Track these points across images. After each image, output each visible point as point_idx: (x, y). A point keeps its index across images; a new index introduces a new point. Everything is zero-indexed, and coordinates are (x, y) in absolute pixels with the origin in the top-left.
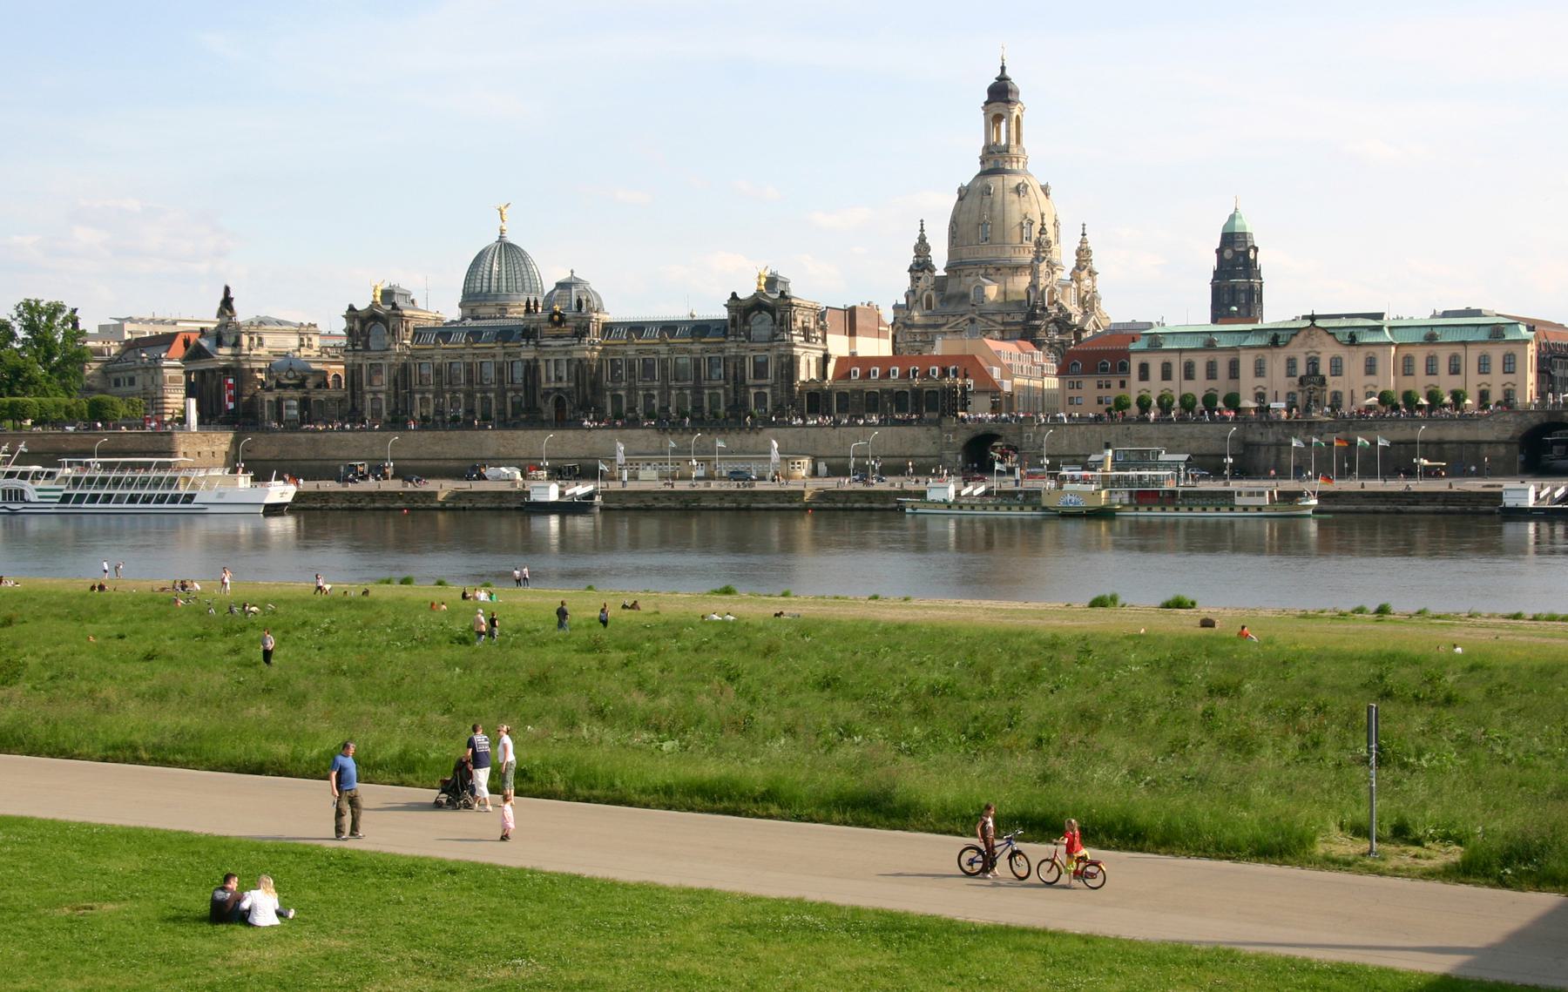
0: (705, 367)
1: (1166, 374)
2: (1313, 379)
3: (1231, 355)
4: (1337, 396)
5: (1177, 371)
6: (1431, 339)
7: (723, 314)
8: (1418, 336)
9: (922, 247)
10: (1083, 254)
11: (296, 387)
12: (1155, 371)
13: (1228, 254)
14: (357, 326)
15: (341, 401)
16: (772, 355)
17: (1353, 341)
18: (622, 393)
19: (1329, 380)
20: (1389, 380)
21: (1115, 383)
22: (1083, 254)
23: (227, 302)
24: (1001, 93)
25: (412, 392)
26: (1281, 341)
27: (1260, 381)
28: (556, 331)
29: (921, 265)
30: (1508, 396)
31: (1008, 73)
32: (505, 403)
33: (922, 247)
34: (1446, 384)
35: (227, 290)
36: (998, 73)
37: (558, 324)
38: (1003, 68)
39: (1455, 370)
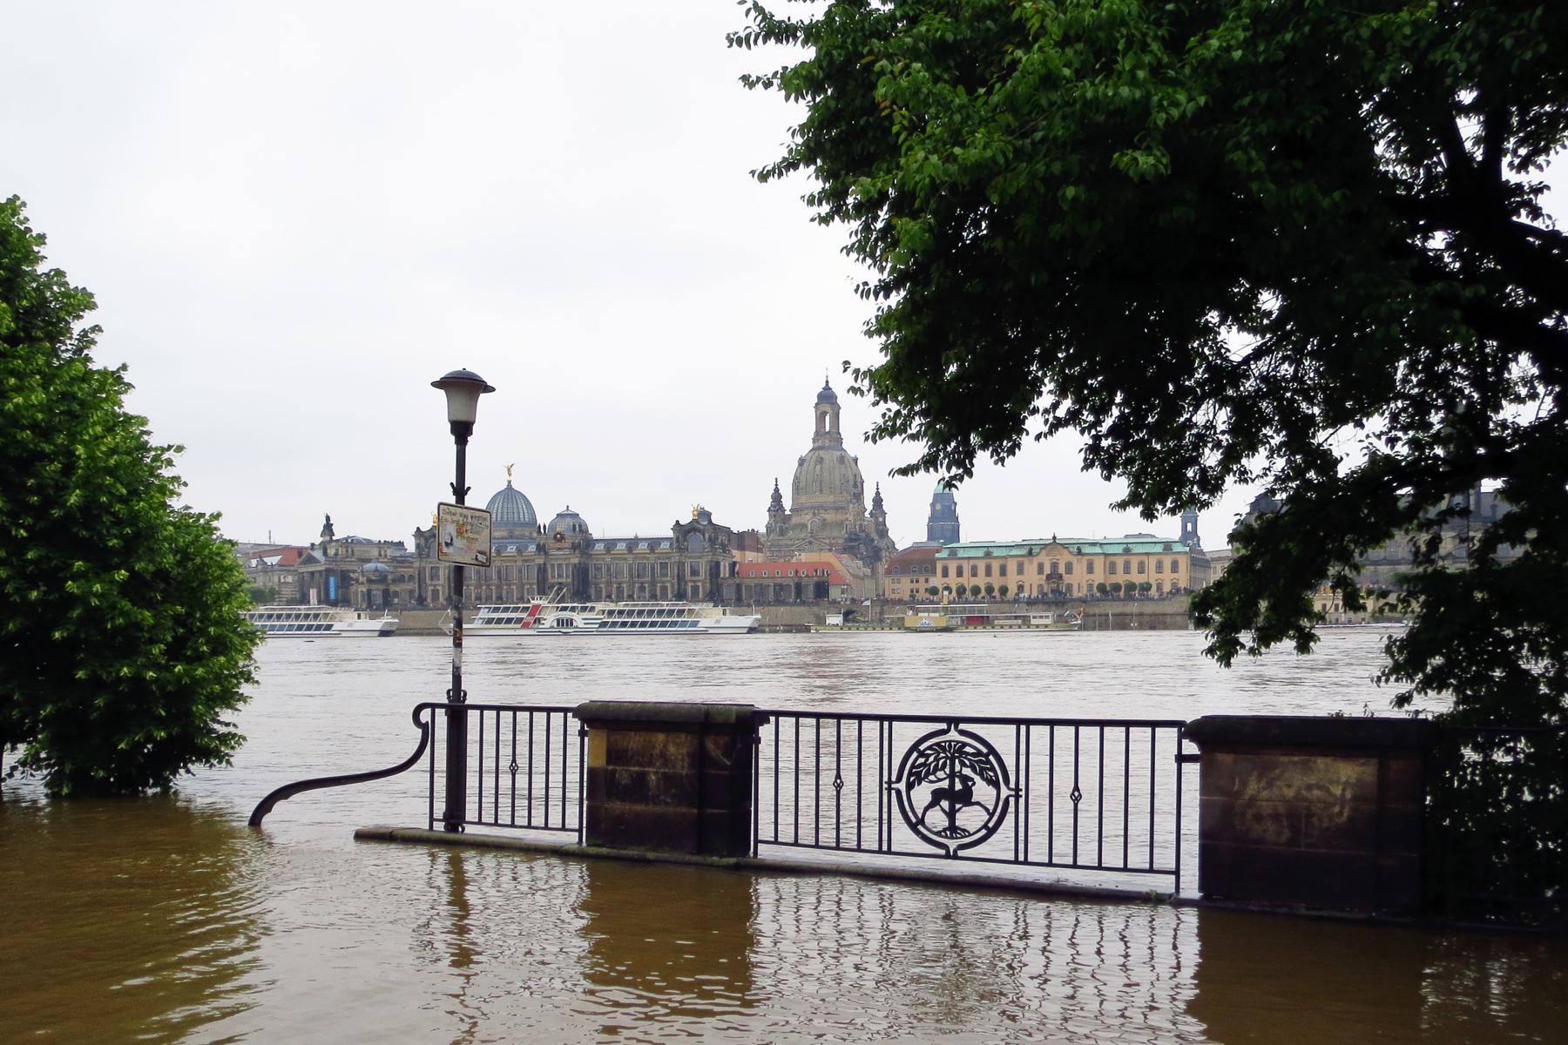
0: (658, 570)
1: (960, 573)
2: (1054, 576)
3: (1002, 562)
4: (1069, 587)
6: (1127, 551)
7: (671, 534)
8: (1119, 549)
9: (777, 497)
10: (878, 501)
12: (952, 571)
13: (938, 507)
14: (422, 542)
15: (411, 592)
16: (703, 561)
17: (1079, 552)
20: (1099, 577)
21: (922, 580)
22: (878, 501)
23: (328, 528)
26: (1035, 550)
27: (1020, 577)
28: (558, 545)
30: (1174, 585)
33: (777, 497)
34: (1138, 579)
35: (328, 518)
37: (559, 541)
39: (1141, 571)
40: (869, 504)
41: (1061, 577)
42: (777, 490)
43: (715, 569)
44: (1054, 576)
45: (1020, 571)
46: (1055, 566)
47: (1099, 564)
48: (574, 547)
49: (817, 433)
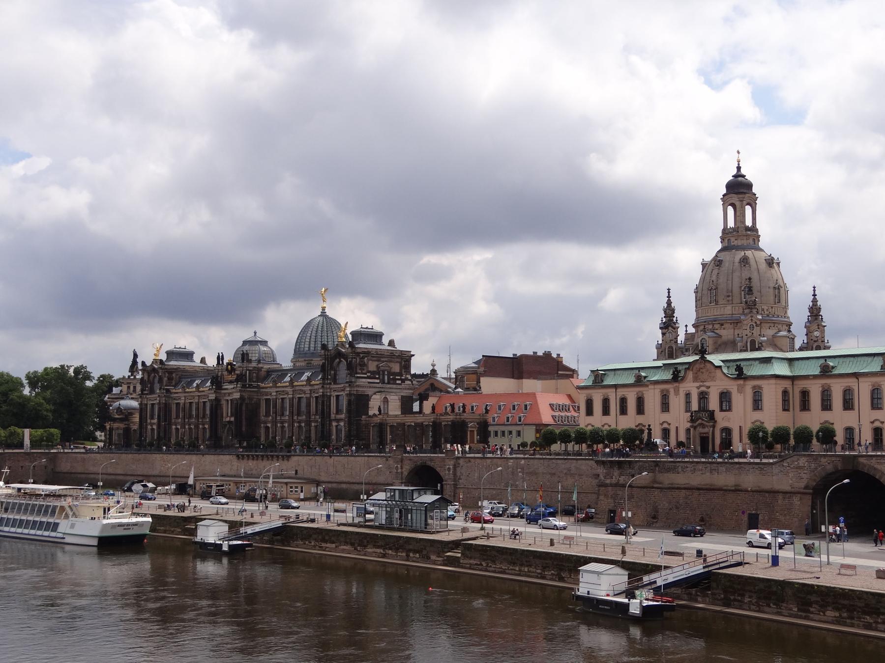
1: (606, 411)
4: (727, 431)
5: (614, 407)
9: (669, 311)
10: (815, 312)
11: (121, 420)
18: (269, 425)
19: (719, 415)
20: (772, 417)
22: (815, 312)
24: (739, 190)
25: (170, 424)
27: (665, 417)
29: (669, 324)
31: (743, 172)
32: (310, 430)
33: (669, 311)
36: (735, 172)
38: (739, 168)
39: (848, 405)
40: (798, 315)
41: (712, 413)
42: (669, 303)
43: (360, 403)
44: (702, 416)
45: (665, 406)
46: (703, 397)
47: (771, 395)
48: (240, 378)
49: (726, 231)
